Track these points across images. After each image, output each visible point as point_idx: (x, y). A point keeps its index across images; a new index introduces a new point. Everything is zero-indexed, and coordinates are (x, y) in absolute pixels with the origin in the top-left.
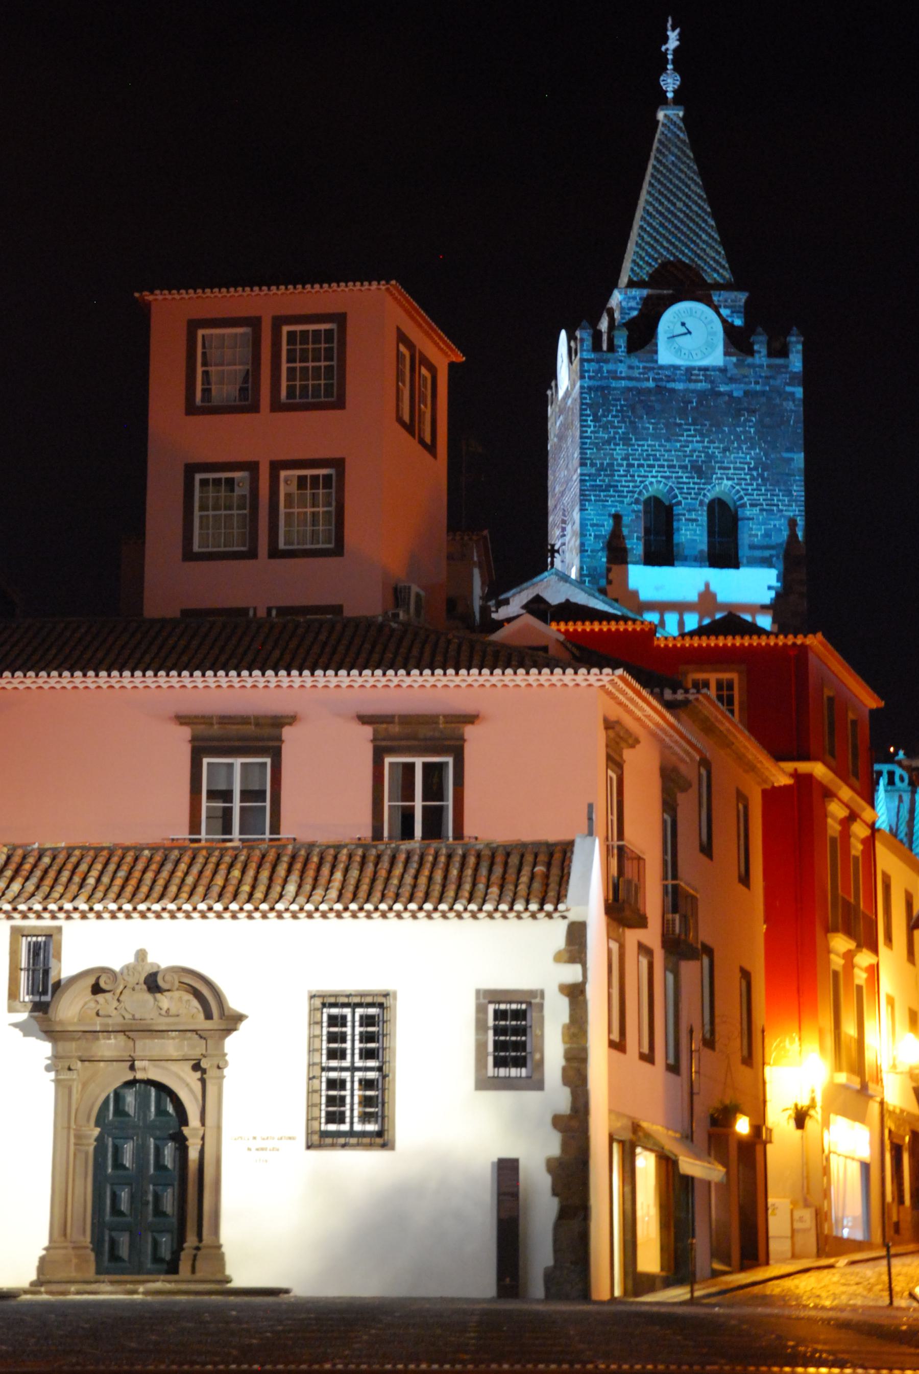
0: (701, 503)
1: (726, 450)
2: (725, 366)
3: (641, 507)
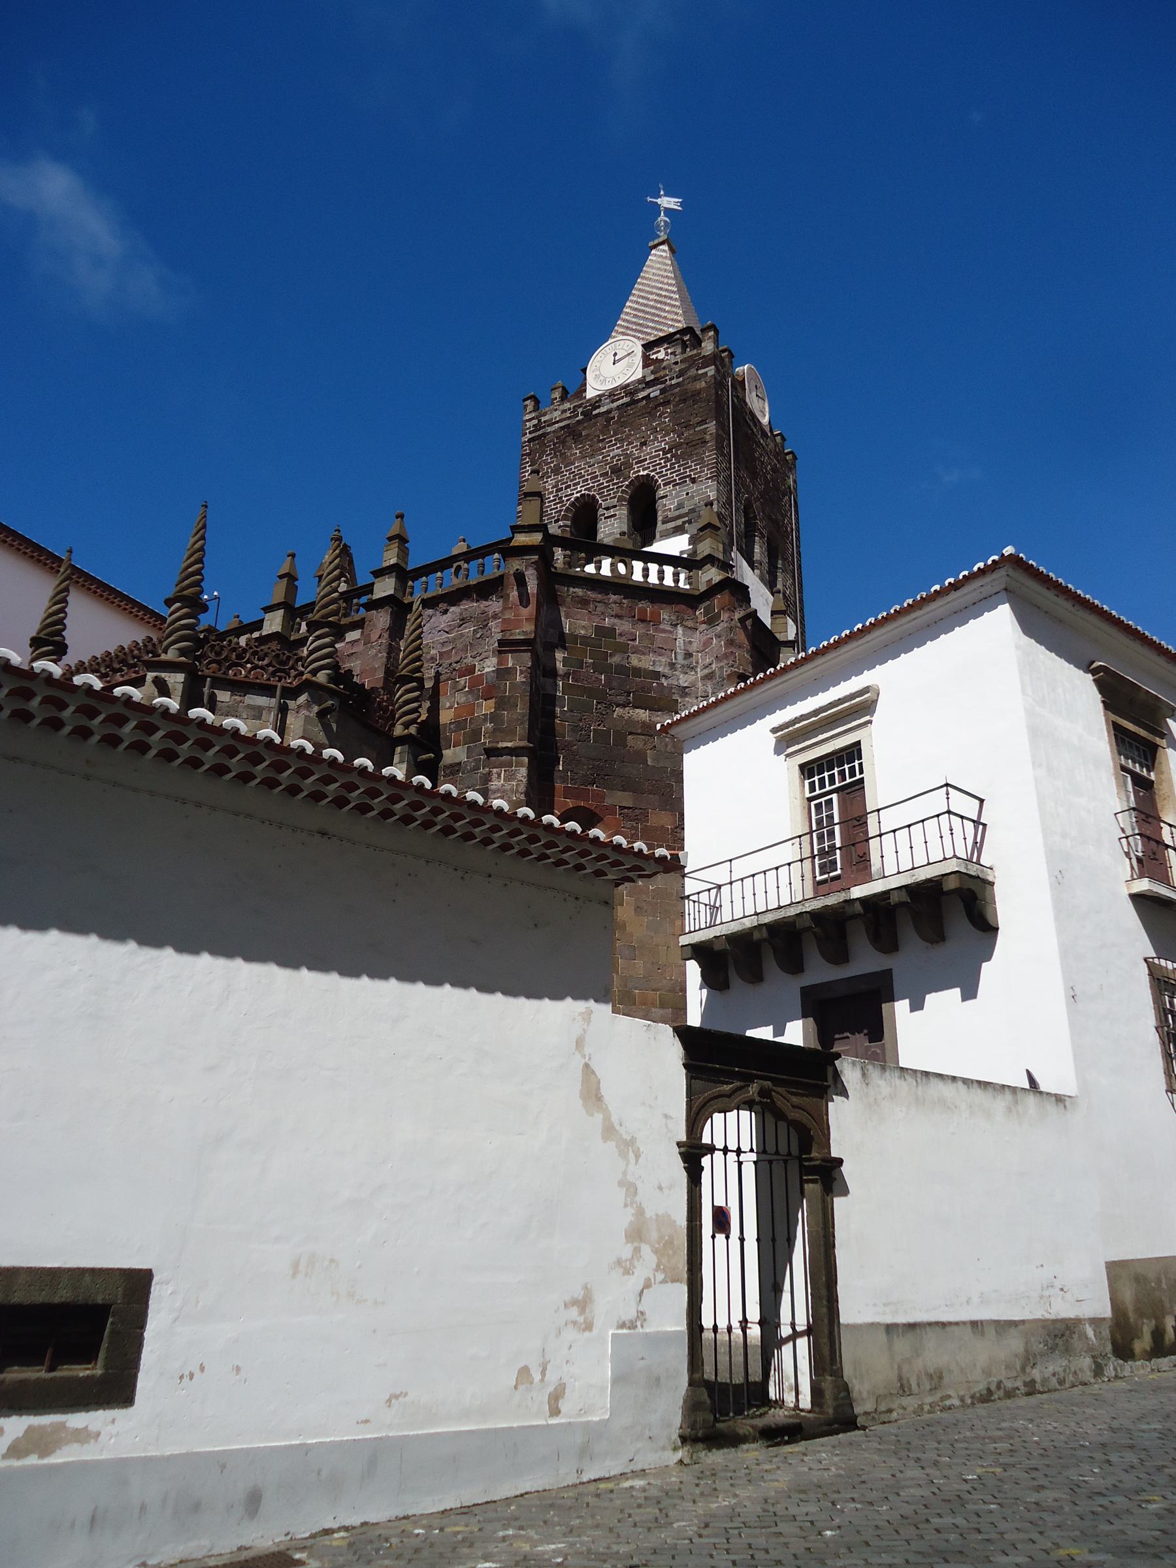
0: (620, 499)
1: (644, 444)
2: (644, 377)
3: (569, 523)
